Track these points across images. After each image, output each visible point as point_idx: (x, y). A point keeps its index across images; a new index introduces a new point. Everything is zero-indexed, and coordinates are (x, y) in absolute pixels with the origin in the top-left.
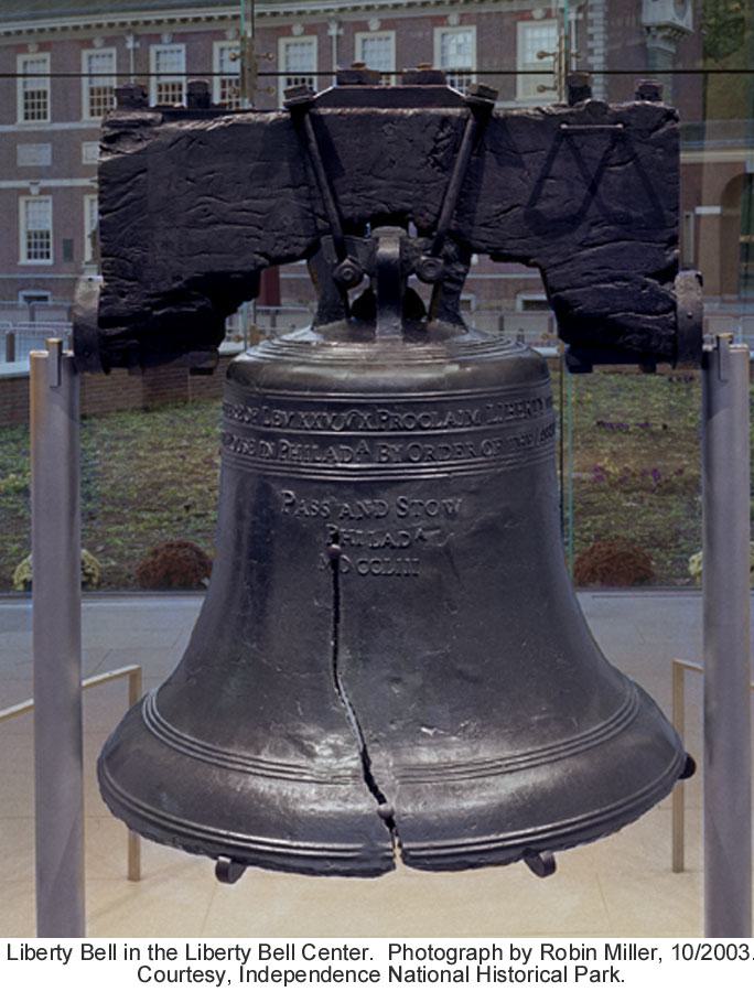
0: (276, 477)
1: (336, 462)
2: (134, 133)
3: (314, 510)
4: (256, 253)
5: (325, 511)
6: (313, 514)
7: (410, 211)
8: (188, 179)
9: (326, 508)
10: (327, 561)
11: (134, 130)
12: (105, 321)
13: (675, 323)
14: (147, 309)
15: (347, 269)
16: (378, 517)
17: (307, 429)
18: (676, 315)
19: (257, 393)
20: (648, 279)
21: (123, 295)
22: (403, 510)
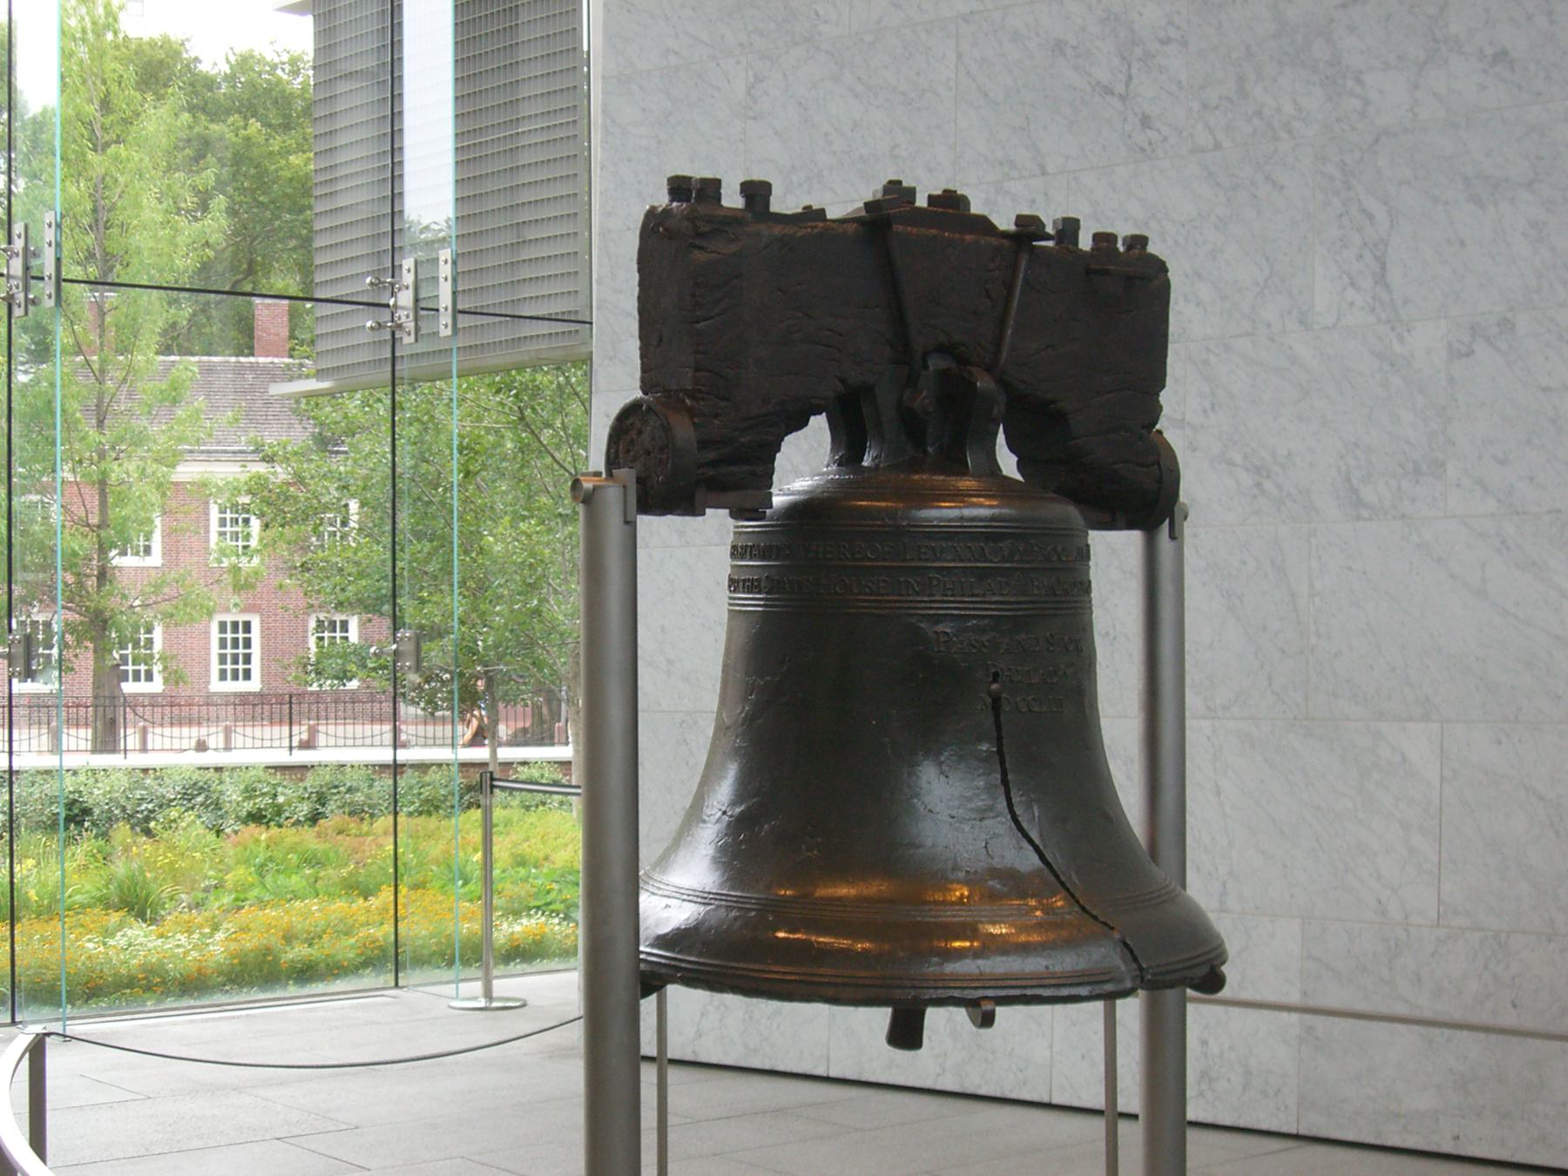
0: (923, 615)
1: (994, 594)
2: (726, 232)
3: (975, 647)
4: (836, 377)
5: (985, 647)
6: (974, 651)
7: (963, 345)
8: (780, 290)
9: (987, 644)
10: (989, 700)
11: (727, 229)
12: (703, 445)
13: (1161, 477)
14: (737, 433)
15: (928, 401)
16: (1034, 651)
17: (962, 561)
18: (1160, 468)
19: (890, 526)
20: (1142, 431)
21: (716, 416)
22: (1052, 644)
